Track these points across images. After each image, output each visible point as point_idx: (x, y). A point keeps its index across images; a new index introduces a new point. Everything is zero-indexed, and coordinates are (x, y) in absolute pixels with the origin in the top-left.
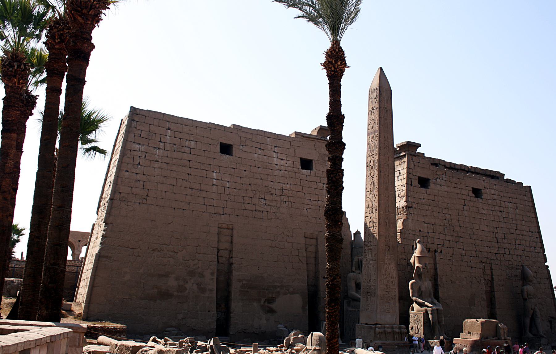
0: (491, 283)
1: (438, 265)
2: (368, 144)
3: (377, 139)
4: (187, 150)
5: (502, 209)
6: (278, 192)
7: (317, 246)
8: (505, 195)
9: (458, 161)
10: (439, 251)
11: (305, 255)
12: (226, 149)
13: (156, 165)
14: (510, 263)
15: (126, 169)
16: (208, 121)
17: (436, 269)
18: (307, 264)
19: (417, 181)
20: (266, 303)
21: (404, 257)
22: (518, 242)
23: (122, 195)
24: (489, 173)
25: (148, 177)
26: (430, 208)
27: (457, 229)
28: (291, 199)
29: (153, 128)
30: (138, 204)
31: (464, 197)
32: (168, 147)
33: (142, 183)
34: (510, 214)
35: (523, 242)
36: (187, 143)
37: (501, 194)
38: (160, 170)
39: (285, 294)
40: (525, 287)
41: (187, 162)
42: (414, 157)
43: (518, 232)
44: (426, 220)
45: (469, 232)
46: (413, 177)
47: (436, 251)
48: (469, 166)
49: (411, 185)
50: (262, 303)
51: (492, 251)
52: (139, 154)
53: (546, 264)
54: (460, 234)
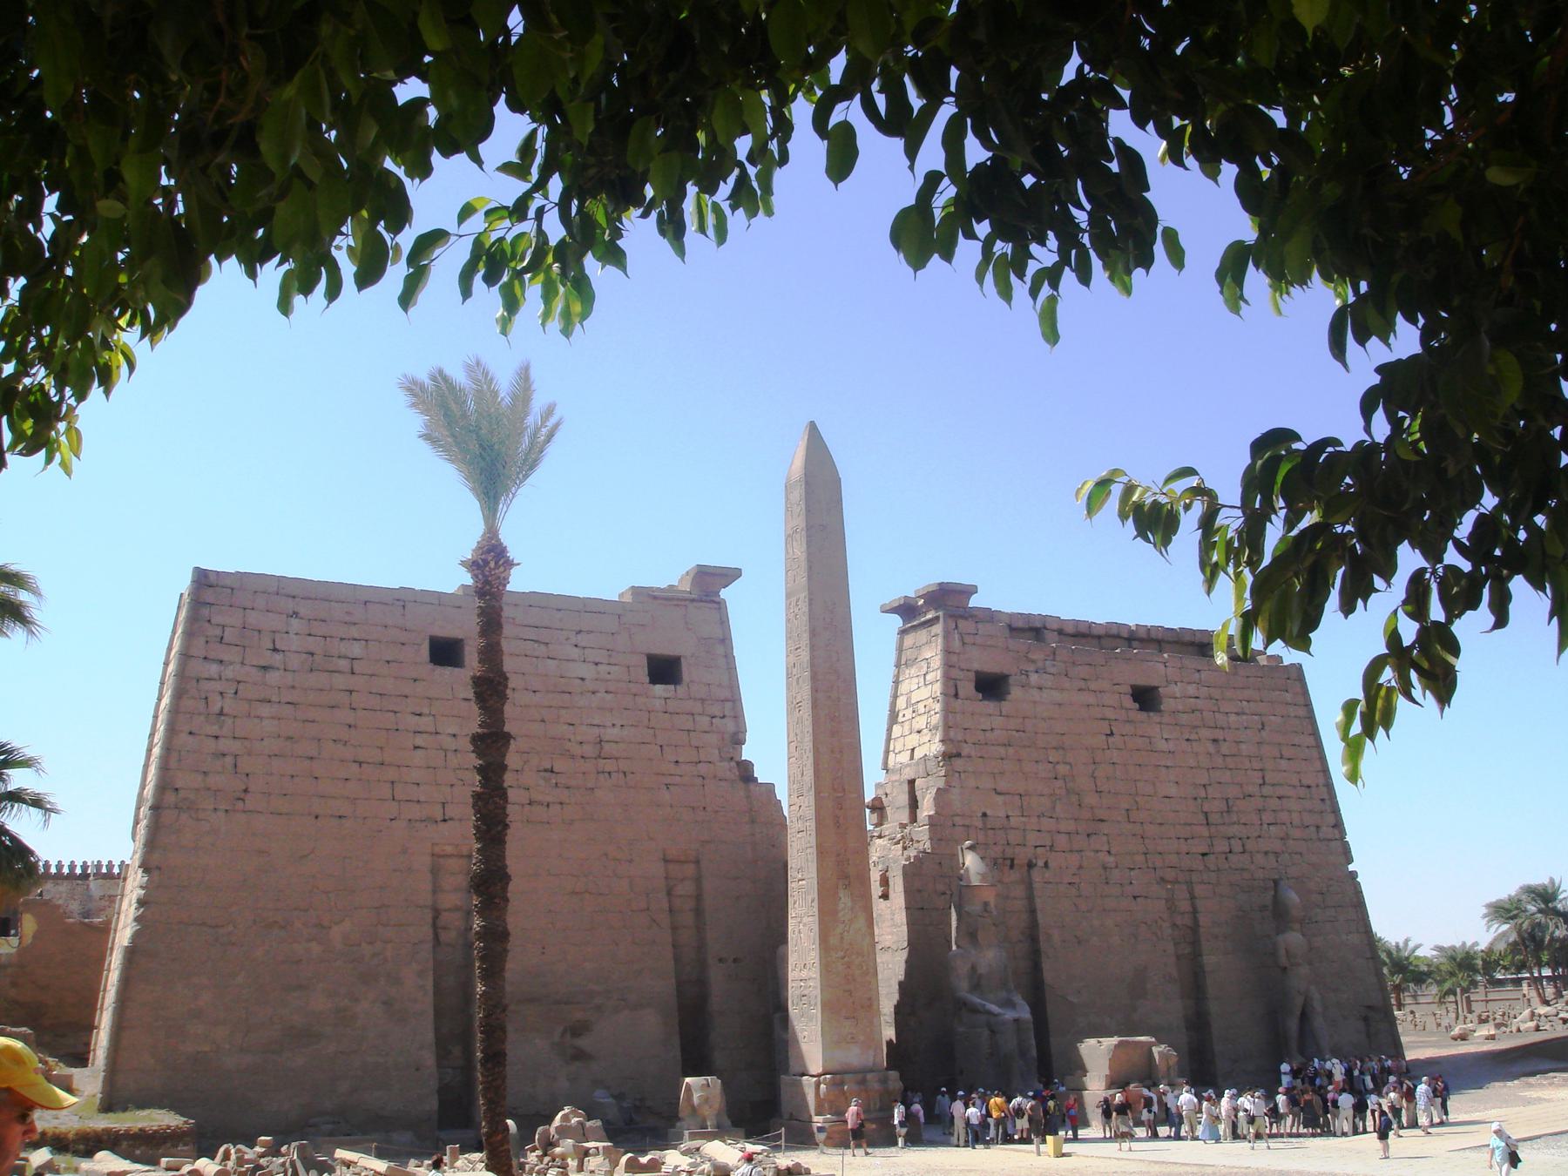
0: (1192, 936)
1: (1039, 903)
2: (788, 621)
3: (806, 609)
4: (343, 664)
5: (1219, 734)
6: (588, 750)
7: (698, 880)
8: (1228, 694)
9: (1098, 613)
10: (1041, 863)
11: (666, 906)
13: (265, 710)
14: (1246, 875)
15: (187, 728)
16: (394, 584)
17: (1033, 911)
18: (674, 928)
20: (568, 1036)
21: (940, 887)
23: (182, 794)
24: (1187, 638)
25: (247, 743)
26: (1011, 750)
27: (1091, 799)
28: (623, 765)
29: (253, 618)
30: (221, 814)
31: (1110, 713)
32: (295, 661)
33: (229, 760)
34: (1243, 746)
35: (1284, 816)
36: (344, 648)
37: (1216, 693)
38: (276, 722)
40: (1280, 938)
42: (961, 623)
43: (1266, 790)
44: (1003, 785)
46: (960, 675)
47: (1030, 865)
48: (1131, 624)
49: (956, 696)
51: (1194, 850)
52: (218, 686)
53: (1351, 868)
54: (1100, 814)
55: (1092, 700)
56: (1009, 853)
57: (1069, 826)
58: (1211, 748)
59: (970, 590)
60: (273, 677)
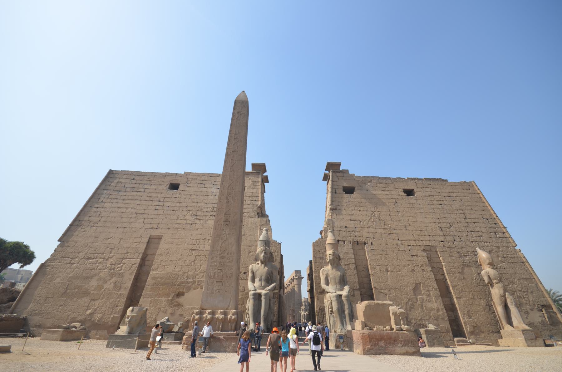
6: (209, 210)
10: (369, 242)
12: (174, 187)
19: (342, 190)
22: (470, 229)
26: (356, 208)
31: (394, 197)
33: (99, 213)
35: (478, 229)
39: (195, 289)
41: (139, 198)
42: (338, 174)
45: (404, 224)
47: (365, 243)
49: (336, 193)
50: (170, 298)
54: (393, 227)
55: (388, 193)
56: (356, 239)
57: (380, 231)
58: (440, 207)
59: (339, 165)
60: (121, 193)
